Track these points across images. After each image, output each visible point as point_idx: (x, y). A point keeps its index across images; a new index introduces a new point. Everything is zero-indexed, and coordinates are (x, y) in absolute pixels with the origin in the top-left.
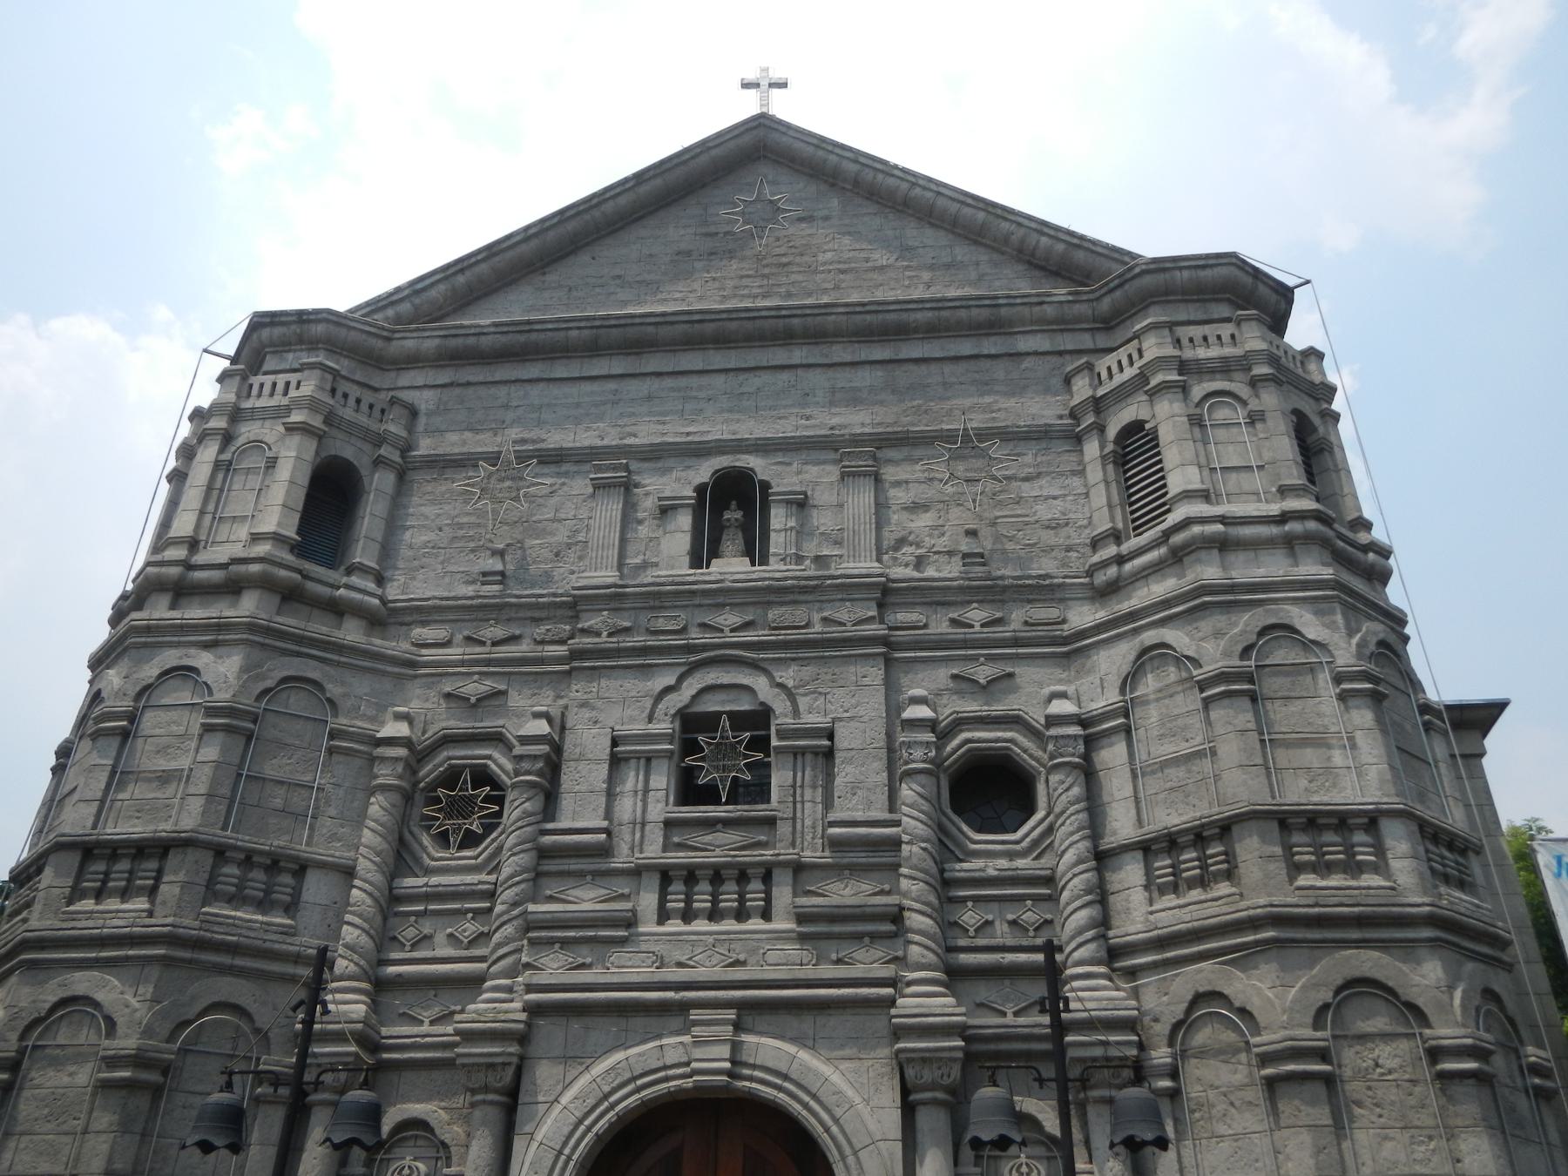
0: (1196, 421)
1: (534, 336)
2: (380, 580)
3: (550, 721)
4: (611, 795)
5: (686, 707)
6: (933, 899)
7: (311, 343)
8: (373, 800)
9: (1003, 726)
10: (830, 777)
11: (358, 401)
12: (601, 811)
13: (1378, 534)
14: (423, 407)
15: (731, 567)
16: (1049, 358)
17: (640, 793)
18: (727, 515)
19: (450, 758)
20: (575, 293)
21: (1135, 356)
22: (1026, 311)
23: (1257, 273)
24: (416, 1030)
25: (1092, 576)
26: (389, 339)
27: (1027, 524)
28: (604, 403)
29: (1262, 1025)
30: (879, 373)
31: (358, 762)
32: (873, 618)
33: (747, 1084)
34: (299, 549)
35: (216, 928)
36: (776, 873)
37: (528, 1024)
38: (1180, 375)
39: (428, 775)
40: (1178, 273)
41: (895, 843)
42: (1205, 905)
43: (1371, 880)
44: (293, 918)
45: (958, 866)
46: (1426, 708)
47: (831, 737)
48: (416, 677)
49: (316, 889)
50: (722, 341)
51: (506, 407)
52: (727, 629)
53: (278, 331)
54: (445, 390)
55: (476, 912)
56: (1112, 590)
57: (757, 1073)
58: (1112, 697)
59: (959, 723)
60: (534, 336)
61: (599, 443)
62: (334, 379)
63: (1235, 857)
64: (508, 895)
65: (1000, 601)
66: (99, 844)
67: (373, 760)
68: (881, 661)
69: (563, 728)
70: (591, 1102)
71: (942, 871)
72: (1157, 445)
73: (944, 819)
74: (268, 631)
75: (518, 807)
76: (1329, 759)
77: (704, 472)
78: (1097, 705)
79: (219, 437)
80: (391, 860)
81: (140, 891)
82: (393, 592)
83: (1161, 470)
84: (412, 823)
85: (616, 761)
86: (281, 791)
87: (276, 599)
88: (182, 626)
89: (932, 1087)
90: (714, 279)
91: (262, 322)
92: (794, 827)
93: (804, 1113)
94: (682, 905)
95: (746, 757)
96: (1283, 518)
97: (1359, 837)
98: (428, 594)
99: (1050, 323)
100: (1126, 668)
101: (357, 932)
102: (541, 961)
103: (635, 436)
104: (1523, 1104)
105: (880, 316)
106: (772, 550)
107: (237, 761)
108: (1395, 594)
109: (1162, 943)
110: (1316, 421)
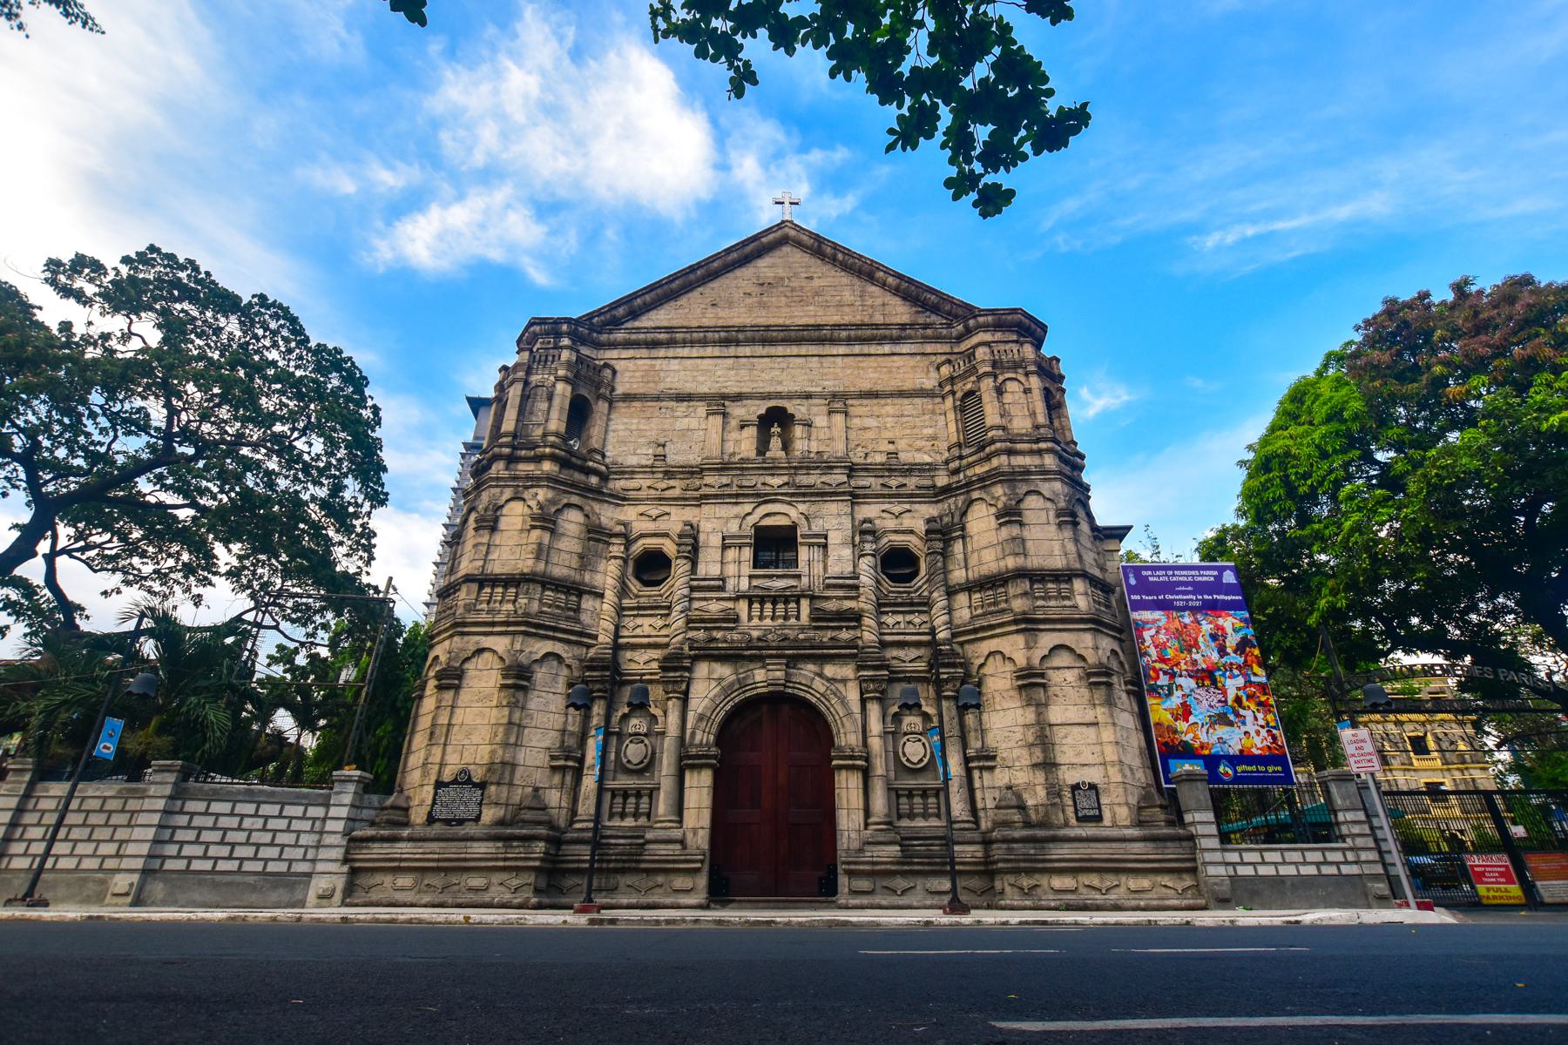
10: (826, 555)
18: (773, 430)
41: (856, 587)
46: (1095, 528)
56: (956, 472)
64: (678, 608)
74: (556, 481)
75: (680, 568)
77: (761, 408)
81: (508, 601)
85: (725, 547)
108: (1086, 477)
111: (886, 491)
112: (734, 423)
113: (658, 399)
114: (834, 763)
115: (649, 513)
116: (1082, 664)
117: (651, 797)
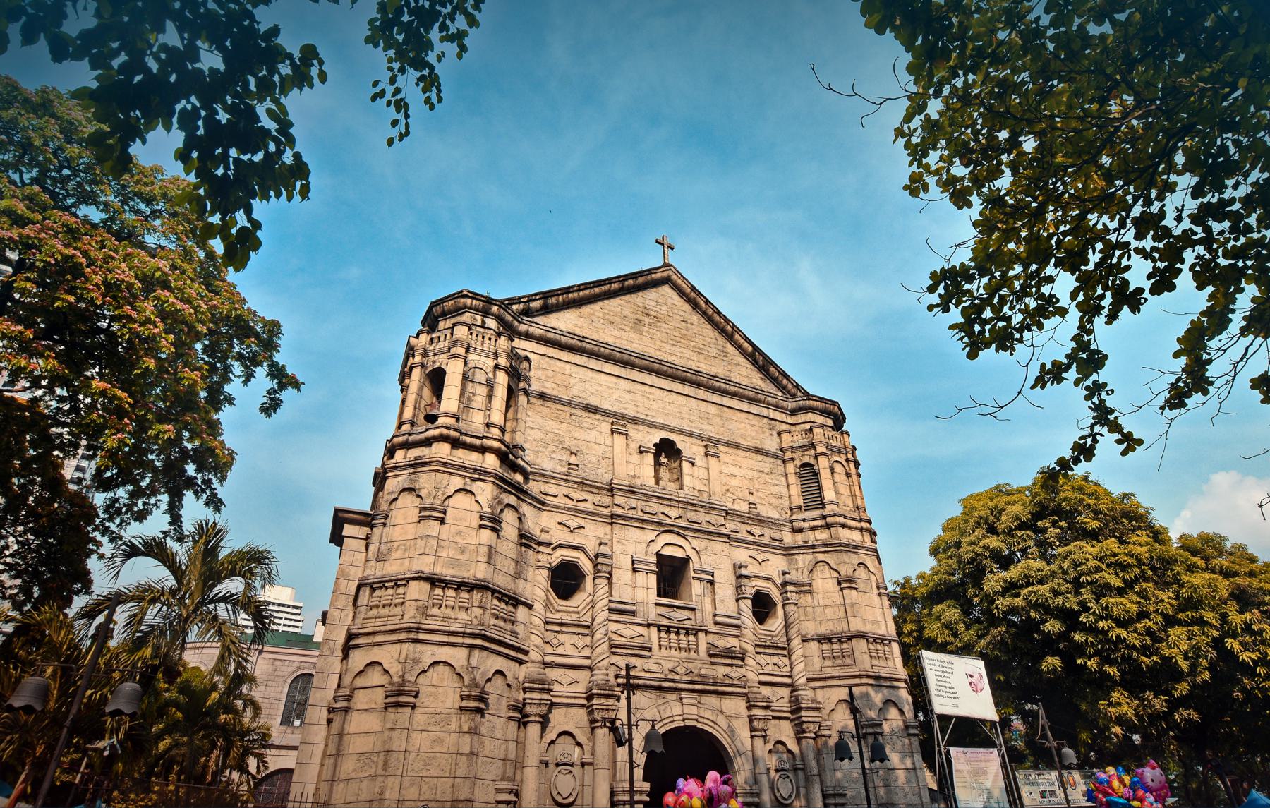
1: (584, 344)
47: (713, 576)
50: (660, 374)
56: (801, 530)
77: (656, 436)
111: (751, 538)
112: (634, 446)
113: (569, 404)
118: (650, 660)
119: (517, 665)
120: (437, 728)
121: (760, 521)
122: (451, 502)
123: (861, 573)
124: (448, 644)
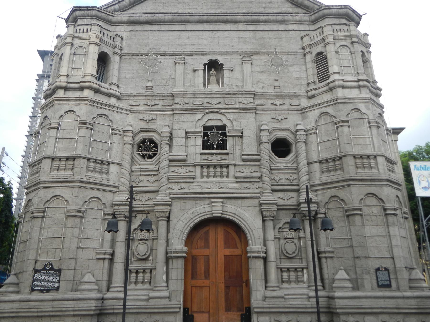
0: (337, 53)
1: (155, 18)
2: (118, 87)
3: (169, 127)
4: (186, 146)
5: (205, 124)
6: (268, 173)
7: (91, 16)
8: (124, 146)
9: (285, 131)
10: (242, 143)
11: (107, 35)
12: (184, 151)
13: (379, 85)
14: (124, 37)
15: (213, 87)
16: (297, 32)
17: (194, 146)
18: (211, 72)
19: (143, 136)
20: (165, 5)
21: (321, 33)
22: (291, 18)
23: (354, 11)
24: (141, 203)
25: (307, 93)
26: (113, 16)
27: (291, 78)
28: (176, 39)
29: (347, 203)
30: (252, 34)
31: (119, 137)
32: (252, 102)
33: (226, 216)
34: (97, 79)
35: (90, 179)
36: (230, 166)
37: (171, 202)
38: (334, 40)
39: (137, 140)
40: (333, 10)
42: (335, 176)
43: (374, 171)
44: (108, 176)
45: (274, 165)
46: (387, 130)
47: (242, 133)
48: (131, 114)
49: (113, 168)
50: (208, 22)
51: (148, 38)
52: (214, 104)
53: (82, 12)
54: (130, 32)
55: (154, 175)
56: (313, 96)
57: (228, 213)
58: (313, 125)
59: (274, 130)
60: (155, 18)
61: (175, 50)
62: (101, 29)
63: (342, 165)
65: (284, 99)
66: (56, 157)
67: (124, 136)
68: (255, 113)
69: (172, 129)
70: (188, 220)
71: (270, 167)
72: (326, 59)
73: (271, 155)
75: (164, 149)
76: (366, 142)
77: (205, 60)
78: (309, 127)
79: (70, 45)
80: (130, 162)
81: (69, 169)
82: (122, 90)
83: (327, 65)
84: (134, 152)
85: (187, 137)
86: (101, 144)
87: (93, 92)
88: (69, 99)
89: (270, 216)
90: (205, 2)
91: (75, 10)
92: (234, 156)
93: (240, 222)
94: (207, 174)
95: (220, 137)
96: (358, 81)
97: (372, 161)
98: (132, 92)
99: (298, 22)
100: (316, 117)
101: (125, 180)
102: (173, 187)
103: (186, 49)
104: (401, 220)
105: (253, 17)
106: (225, 83)
107: (89, 136)
108: (382, 100)
109: (323, 184)
110: (366, 53)
111: (274, 107)
112: (191, 68)
114: (249, 255)
115: (145, 119)
116: (382, 204)
117: (151, 272)
118: (194, 184)
119: (112, 194)
120: (56, 226)
121: (281, 96)
122: (65, 118)
123: (356, 115)
124: (61, 187)
